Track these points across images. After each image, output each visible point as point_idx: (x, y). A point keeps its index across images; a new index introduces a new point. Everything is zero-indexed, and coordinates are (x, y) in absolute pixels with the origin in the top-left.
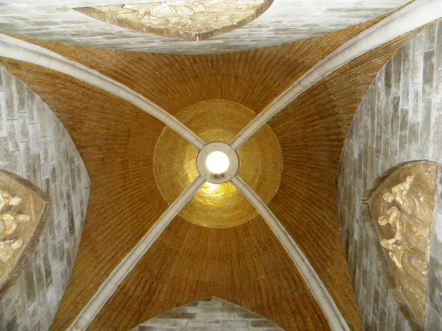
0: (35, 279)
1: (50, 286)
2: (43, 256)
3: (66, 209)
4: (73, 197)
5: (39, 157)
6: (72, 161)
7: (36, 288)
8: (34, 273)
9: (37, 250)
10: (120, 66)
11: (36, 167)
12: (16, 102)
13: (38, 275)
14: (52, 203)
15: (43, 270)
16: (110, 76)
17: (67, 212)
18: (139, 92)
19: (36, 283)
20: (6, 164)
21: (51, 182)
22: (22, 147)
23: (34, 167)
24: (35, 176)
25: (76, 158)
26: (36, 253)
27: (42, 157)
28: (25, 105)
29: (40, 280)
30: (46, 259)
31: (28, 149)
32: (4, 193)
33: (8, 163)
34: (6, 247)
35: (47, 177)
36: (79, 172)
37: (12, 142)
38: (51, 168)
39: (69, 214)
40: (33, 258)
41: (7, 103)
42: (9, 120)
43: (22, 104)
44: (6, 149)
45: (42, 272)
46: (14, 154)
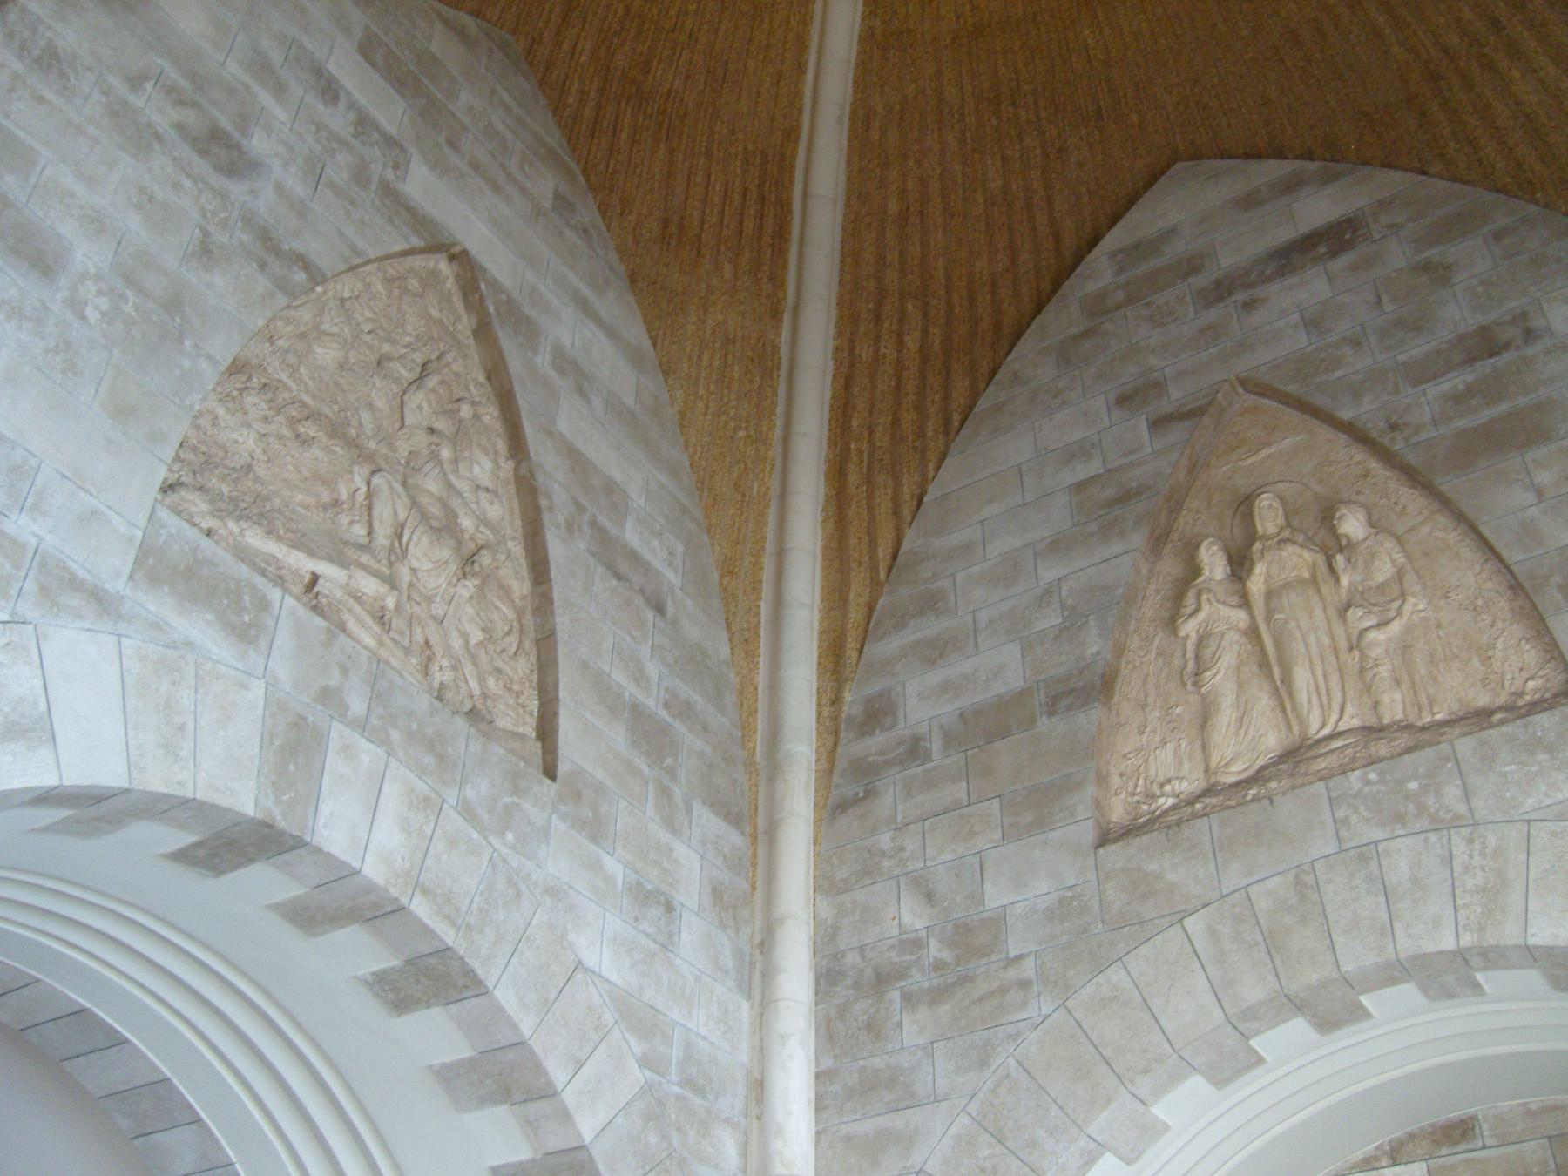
0: (1486, 415)
1: (1537, 323)
2: (1410, 391)
3: (1260, 291)
4: (1227, 260)
5: (1080, 487)
6: (1098, 307)
7: (1522, 401)
8: (1462, 423)
9: (1382, 425)
10: (728, 270)
11: (1111, 492)
12: (929, 627)
13: (1474, 402)
14: (1234, 379)
15: (1458, 380)
16: (778, 281)
17: (1274, 288)
18: (797, 95)
19: (1503, 408)
20: (1094, 631)
21: (1165, 407)
22: (1049, 573)
23: (1111, 503)
24: (1139, 492)
25: (1091, 287)
26: (1394, 427)
27: (1082, 471)
28: (933, 586)
29: (1488, 391)
30: (1422, 373)
31: (1058, 546)
32: (1185, 607)
33: (1092, 623)
34: (1356, 561)
35: (1144, 426)
36: (1140, 250)
37: (1037, 619)
38: (1117, 414)
39: (1281, 273)
40: (1406, 439)
41: (931, 662)
42: (976, 642)
43: (931, 603)
44: (1055, 639)
45: (1470, 378)
46: (1070, 601)
